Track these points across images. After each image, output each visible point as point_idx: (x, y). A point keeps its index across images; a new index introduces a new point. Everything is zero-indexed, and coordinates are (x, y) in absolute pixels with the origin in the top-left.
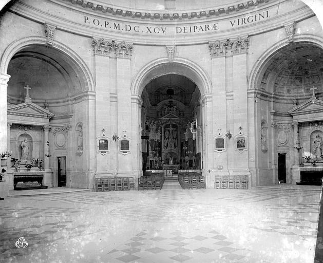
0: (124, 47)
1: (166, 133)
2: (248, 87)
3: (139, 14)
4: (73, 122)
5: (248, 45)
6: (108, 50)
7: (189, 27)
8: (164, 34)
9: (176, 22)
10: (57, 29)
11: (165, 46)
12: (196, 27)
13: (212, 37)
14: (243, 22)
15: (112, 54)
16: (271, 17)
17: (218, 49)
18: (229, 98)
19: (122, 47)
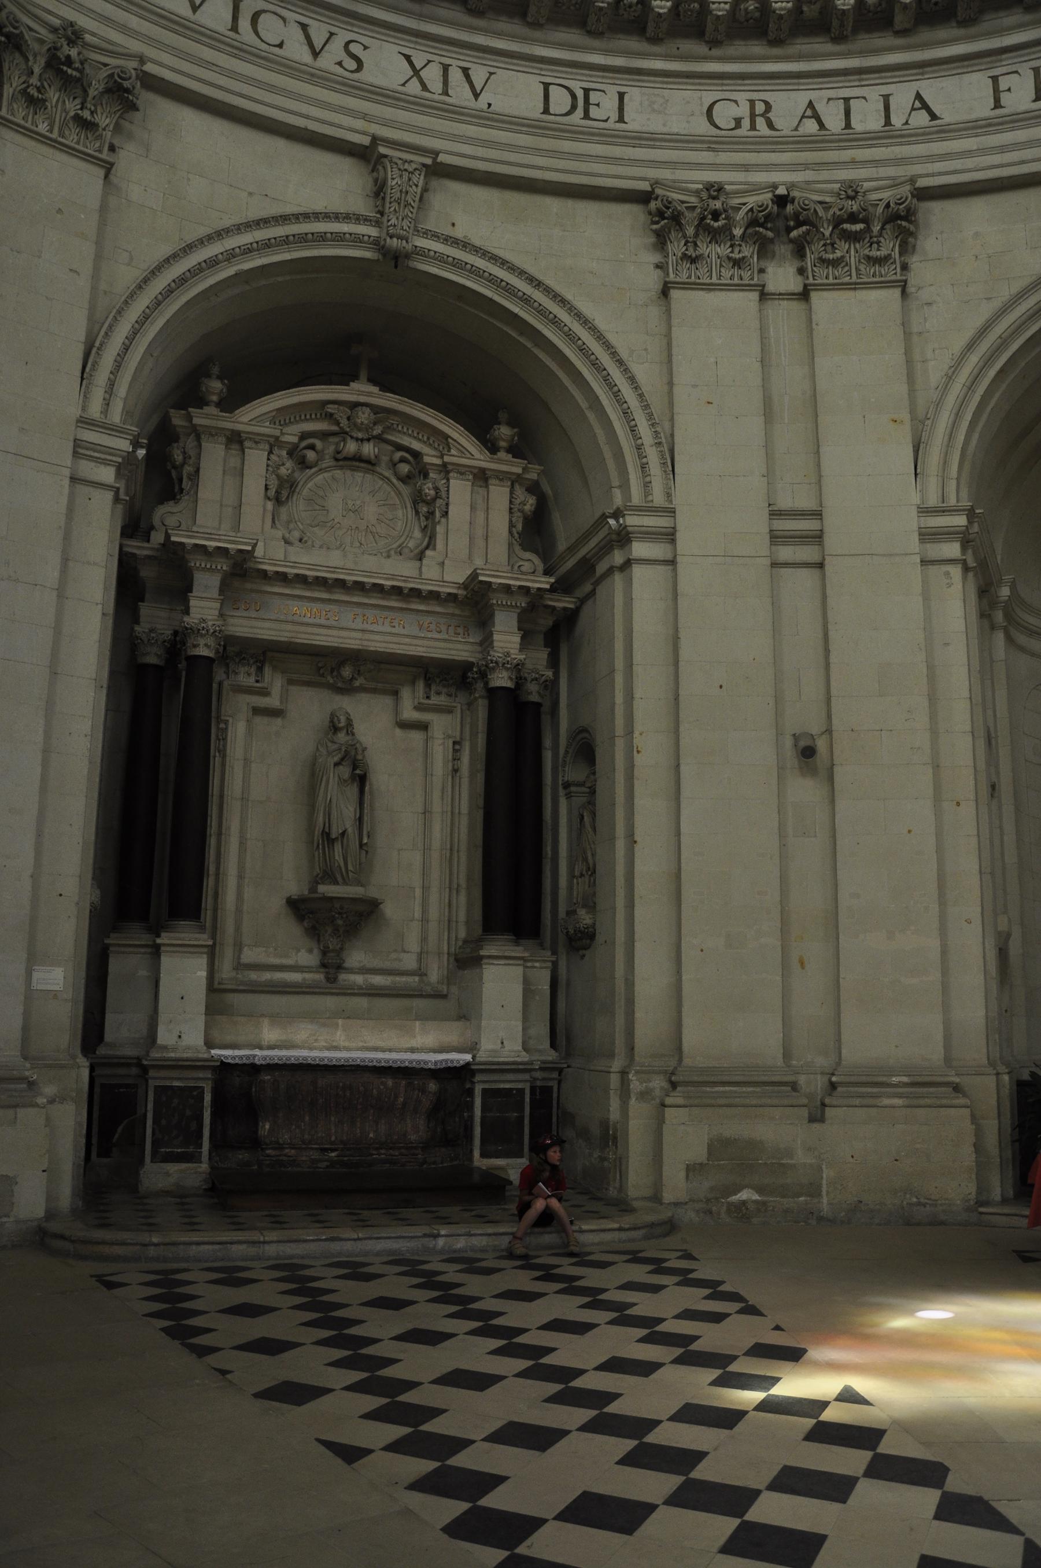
0: (853, 218)
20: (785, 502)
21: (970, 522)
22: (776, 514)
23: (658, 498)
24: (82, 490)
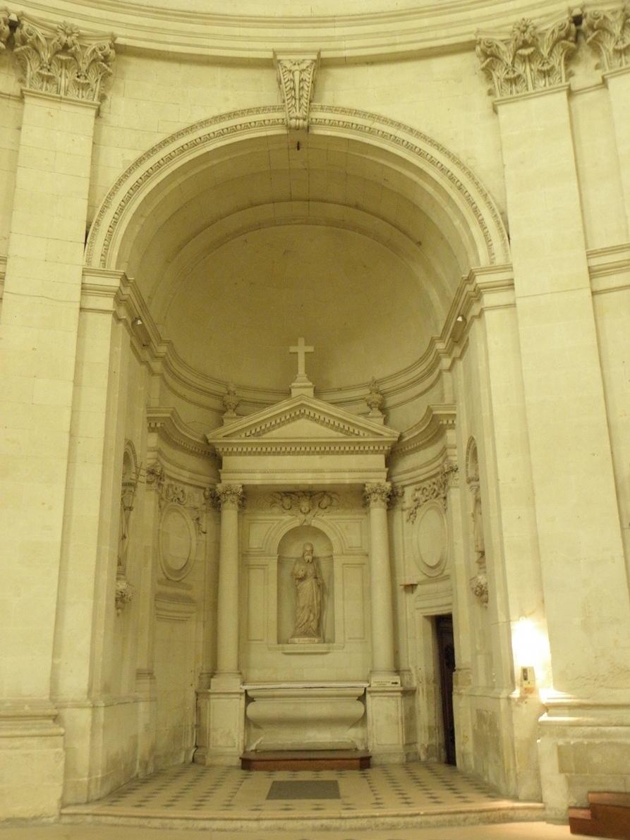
6: (557, 60)
15: (585, 74)
20: (598, 244)
22: (590, 255)
23: (499, 260)
24: (91, 317)
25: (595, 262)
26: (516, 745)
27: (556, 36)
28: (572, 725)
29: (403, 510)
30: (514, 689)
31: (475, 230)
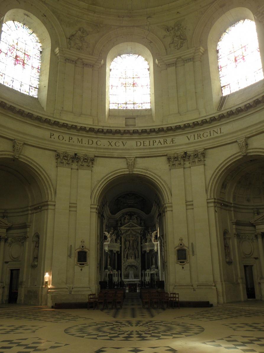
0: (86, 159)
1: (126, 243)
2: (207, 197)
3: (101, 130)
4: (31, 232)
5: (204, 157)
6: (70, 162)
7: (148, 141)
8: (125, 147)
9: (136, 136)
10: (24, 144)
11: (125, 158)
12: (154, 142)
13: (170, 150)
14: (199, 137)
15: (74, 166)
16: (224, 134)
17: (176, 160)
18: (189, 207)
19: (84, 159)
20: (72, 202)
21: (98, 206)
25: (70, 205)
26: (43, 296)
27: (71, 157)
28: (54, 292)
29: (8, 243)
30: (43, 285)
31: (49, 191)
